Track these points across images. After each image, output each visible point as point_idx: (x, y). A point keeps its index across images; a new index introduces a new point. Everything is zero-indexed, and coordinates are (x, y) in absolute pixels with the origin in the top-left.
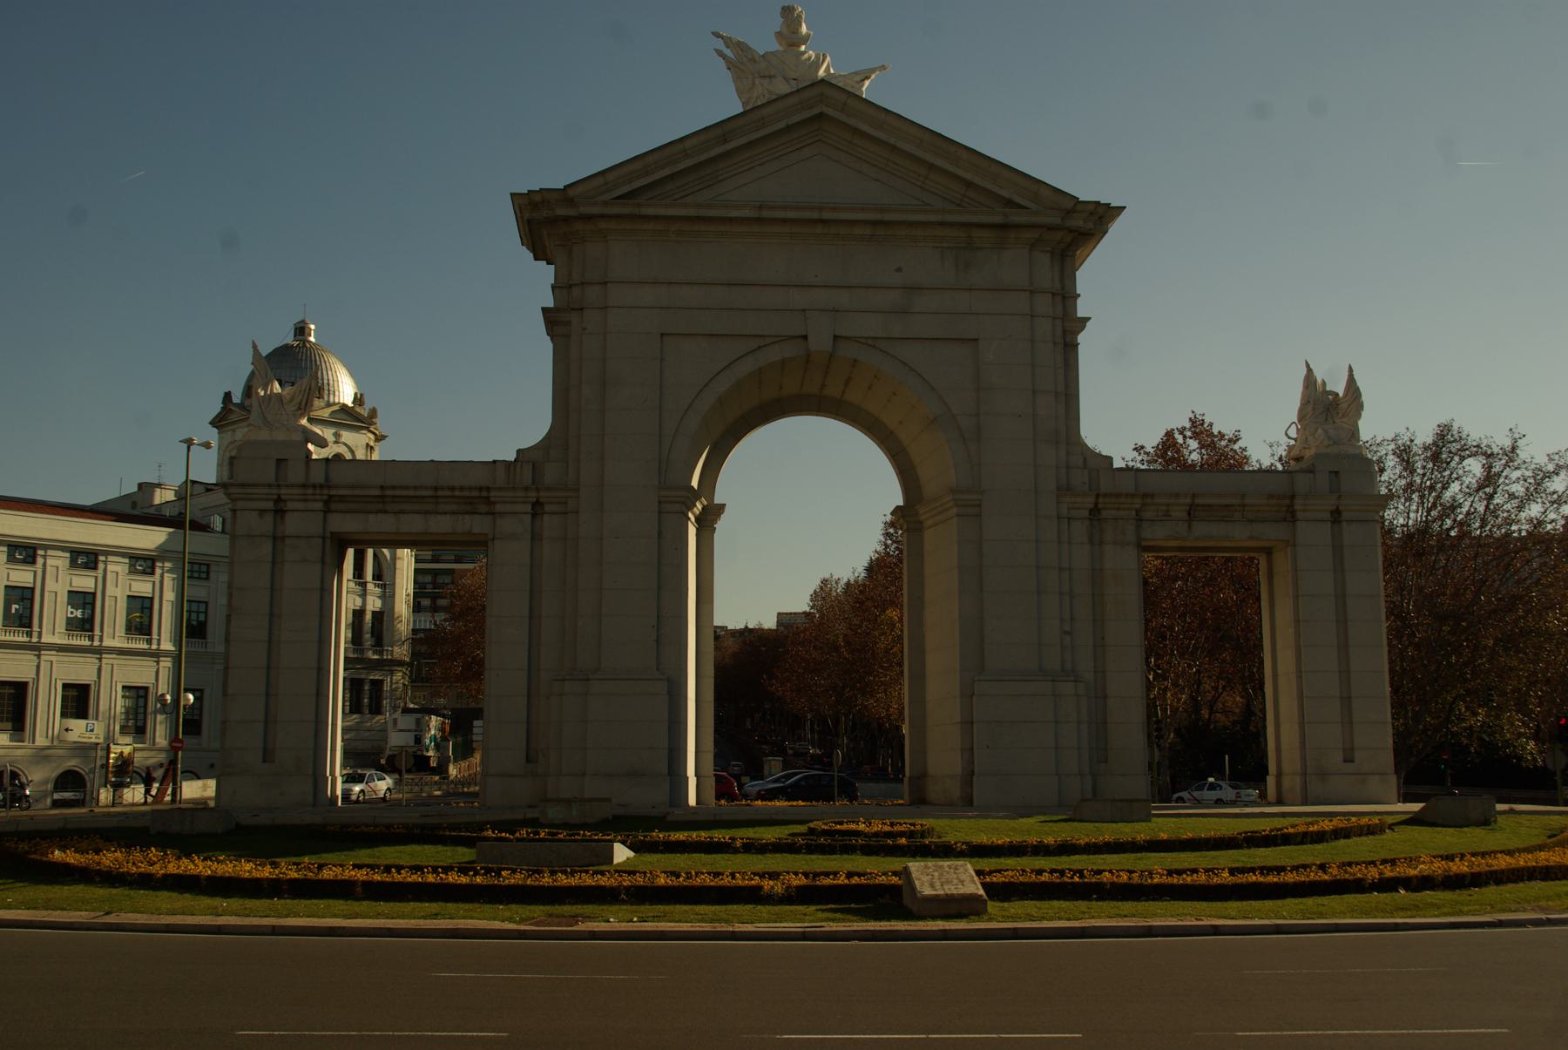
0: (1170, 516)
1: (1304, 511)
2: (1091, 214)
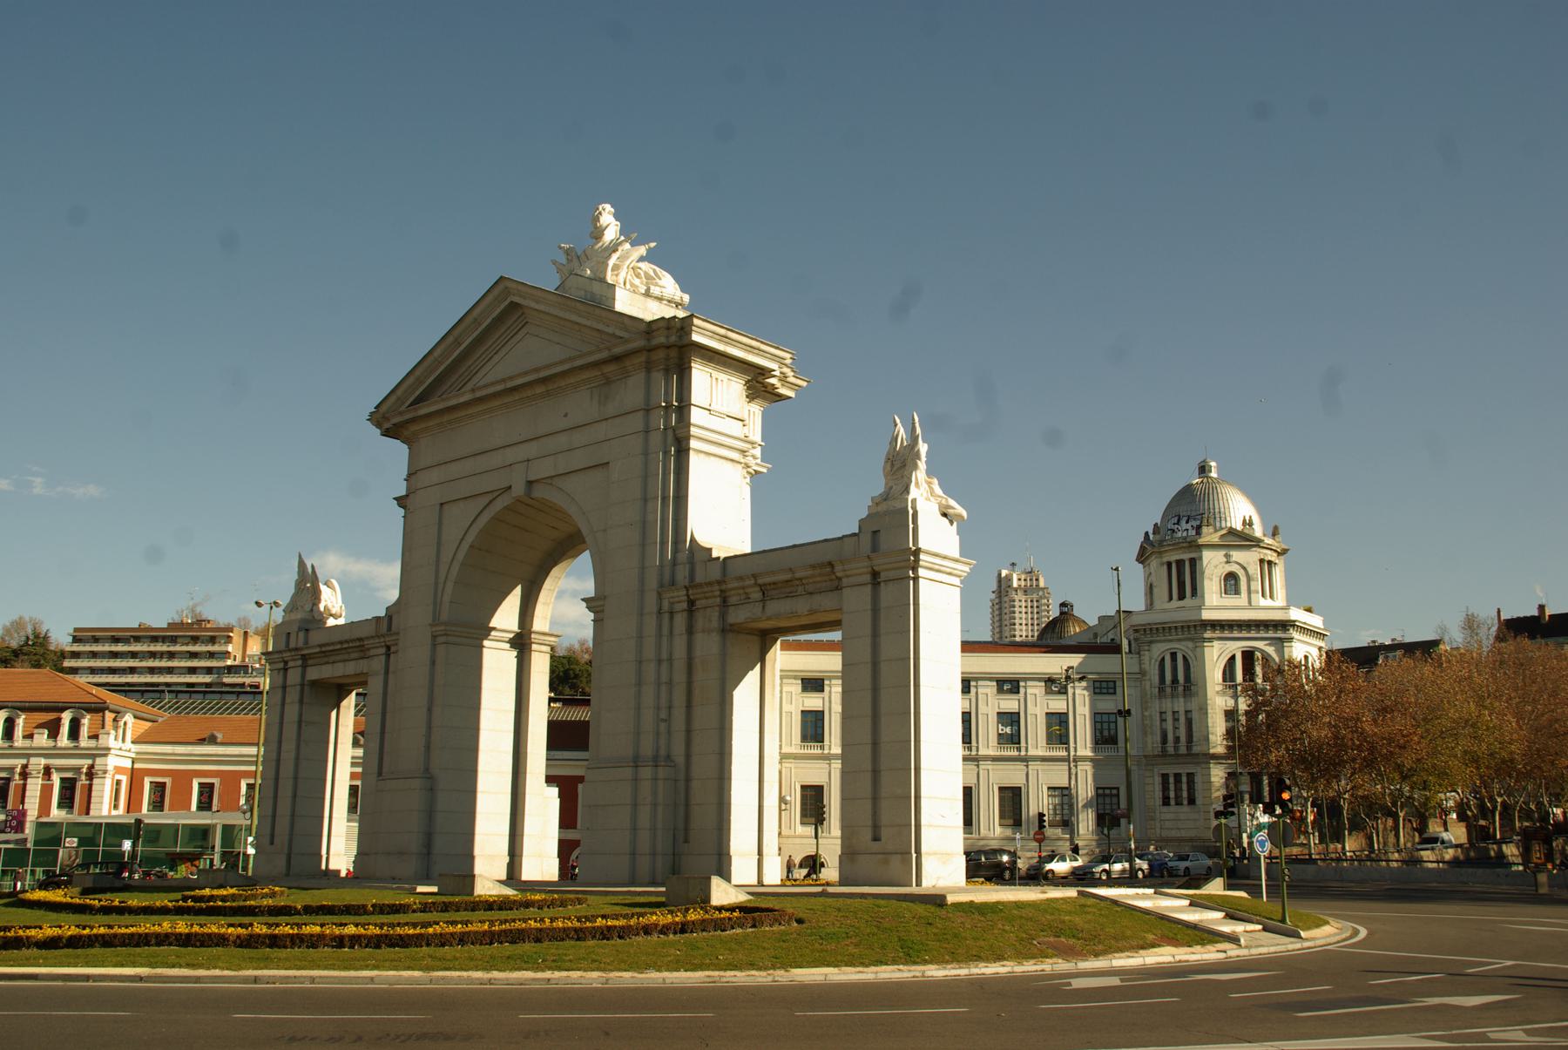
0: (749, 598)
1: (848, 576)
2: (668, 328)
